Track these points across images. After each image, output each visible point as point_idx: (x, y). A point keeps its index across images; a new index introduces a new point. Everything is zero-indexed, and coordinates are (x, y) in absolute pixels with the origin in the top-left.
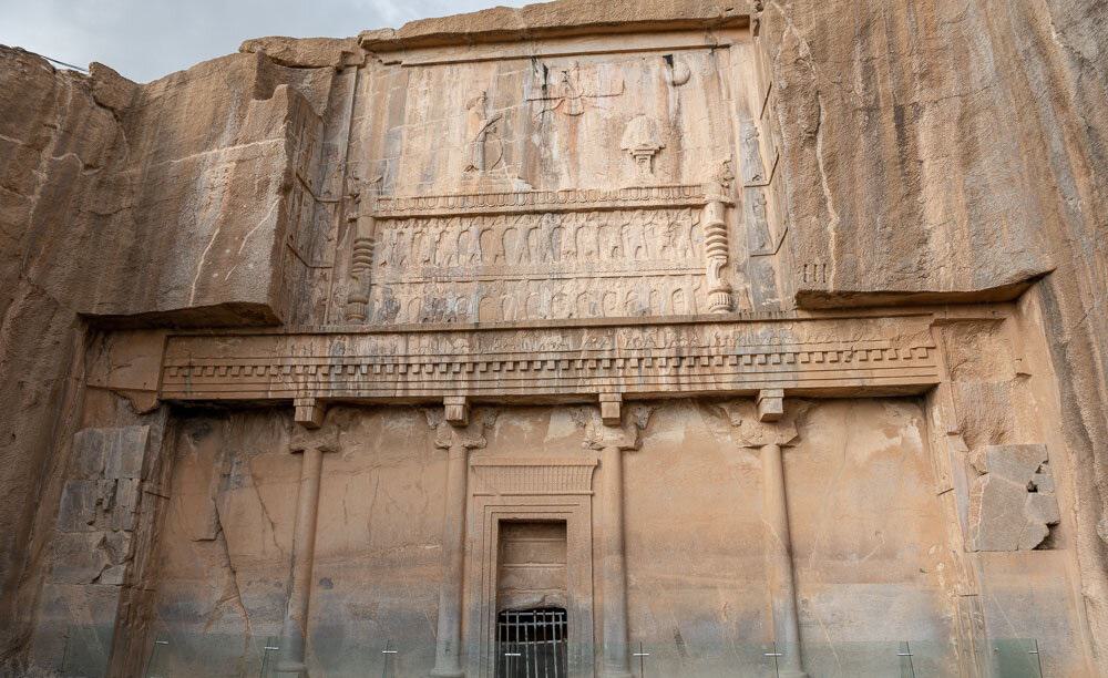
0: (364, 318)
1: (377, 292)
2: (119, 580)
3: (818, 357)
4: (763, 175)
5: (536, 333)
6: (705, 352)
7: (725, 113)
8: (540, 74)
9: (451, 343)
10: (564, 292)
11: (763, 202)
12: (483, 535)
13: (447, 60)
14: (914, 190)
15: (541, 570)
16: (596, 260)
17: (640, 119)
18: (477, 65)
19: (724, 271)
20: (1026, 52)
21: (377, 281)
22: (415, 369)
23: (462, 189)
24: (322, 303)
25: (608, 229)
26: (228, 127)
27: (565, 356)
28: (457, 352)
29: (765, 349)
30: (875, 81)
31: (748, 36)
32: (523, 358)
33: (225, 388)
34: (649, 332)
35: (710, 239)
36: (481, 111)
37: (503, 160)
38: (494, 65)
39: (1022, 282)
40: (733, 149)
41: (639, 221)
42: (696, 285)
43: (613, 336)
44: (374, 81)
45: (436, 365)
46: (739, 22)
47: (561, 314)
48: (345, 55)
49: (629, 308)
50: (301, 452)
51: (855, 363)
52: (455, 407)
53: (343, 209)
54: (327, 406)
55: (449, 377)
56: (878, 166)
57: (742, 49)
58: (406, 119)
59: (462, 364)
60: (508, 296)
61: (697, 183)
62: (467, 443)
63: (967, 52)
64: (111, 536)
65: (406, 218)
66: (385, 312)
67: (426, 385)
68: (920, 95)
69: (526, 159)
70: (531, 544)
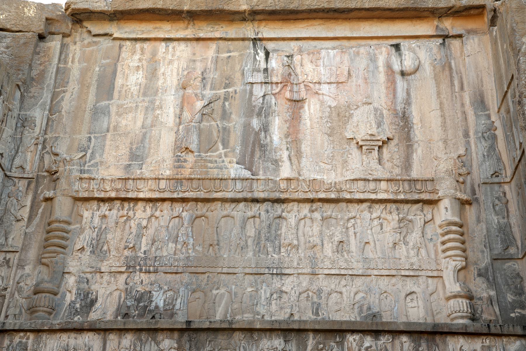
0: (52, 310)
1: (71, 281)
4: (503, 172)
5: (256, 336)
7: (458, 105)
9: (158, 344)
10: (284, 289)
11: (504, 201)
13: (162, 36)
17: (367, 107)
18: (194, 43)
19: (462, 273)
21: (71, 269)
23: (175, 172)
34: (384, 340)
35: (446, 237)
38: (213, 46)
40: (468, 143)
41: (366, 215)
42: (431, 288)
43: (341, 344)
44: (80, 52)
47: (276, 313)
49: (356, 310)
53: (37, 187)
57: (476, 40)
58: (116, 94)
60: (222, 291)
61: (428, 175)
65: (110, 200)
66: (78, 306)
69: (245, 142)
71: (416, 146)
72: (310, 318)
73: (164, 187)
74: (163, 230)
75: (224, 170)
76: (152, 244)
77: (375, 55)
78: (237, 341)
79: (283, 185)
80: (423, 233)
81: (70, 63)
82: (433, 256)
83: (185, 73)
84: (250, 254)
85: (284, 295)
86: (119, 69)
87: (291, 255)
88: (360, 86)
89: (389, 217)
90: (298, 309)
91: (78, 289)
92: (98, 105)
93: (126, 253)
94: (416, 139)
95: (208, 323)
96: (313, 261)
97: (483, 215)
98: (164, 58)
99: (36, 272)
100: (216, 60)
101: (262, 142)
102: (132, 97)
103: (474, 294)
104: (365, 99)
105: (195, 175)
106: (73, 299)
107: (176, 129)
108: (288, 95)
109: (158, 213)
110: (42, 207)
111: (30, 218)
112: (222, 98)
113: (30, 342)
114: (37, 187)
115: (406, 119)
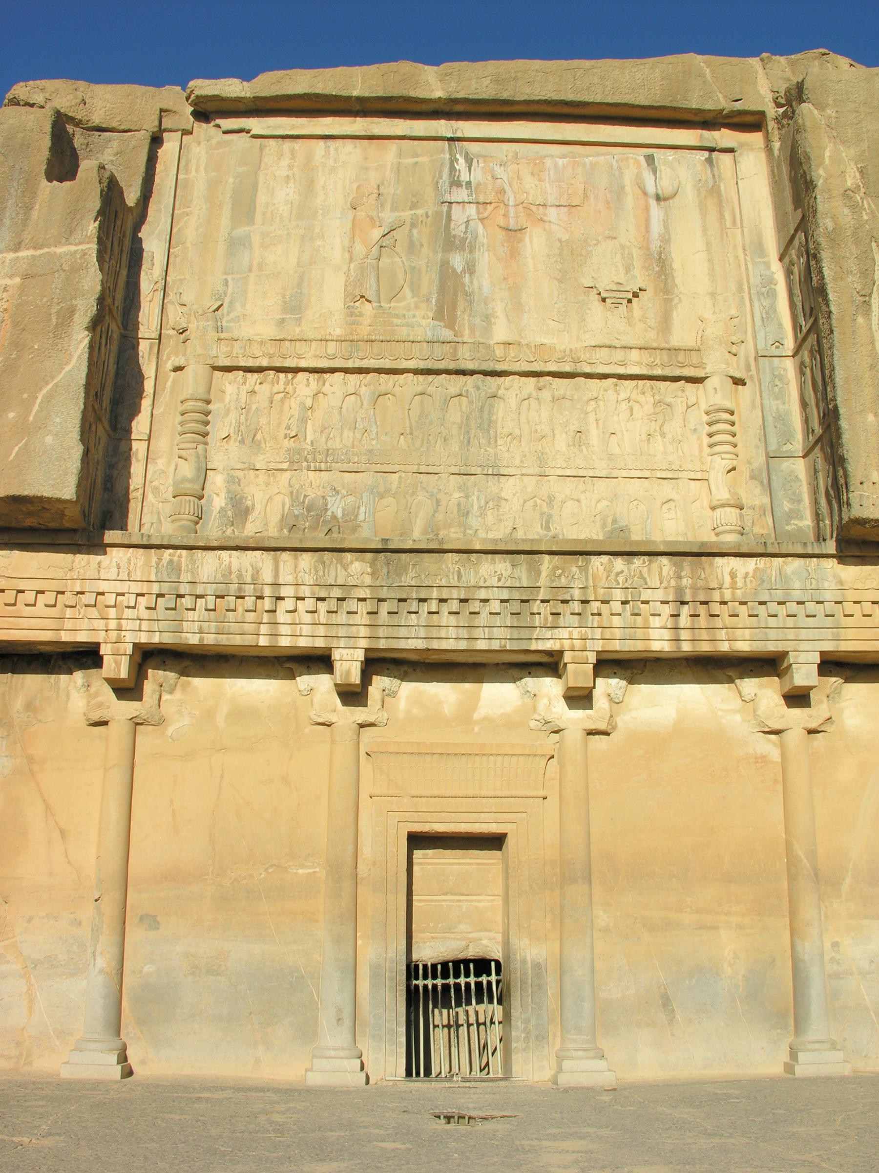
1: (217, 481)
6: (716, 596)
8: (462, 161)
9: (345, 567)
10: (503, 495)
15: (464, 906)
27: (516, 595)
29: (797, 595)
32: (455, 594)
38: (393, 145)
41: (611, 395)
43: (584, 569)
46: (748, 119)
49: (598, 524)
65: (260, 370)
66: (230, 513)
67: (306, 630)
71: (676, 300)
72: (538, 533)
73: (333, 352)
74: (336, 412)
75: (416, 328)
76: (322, 432)
77: (619, 168)
78: (450, 565)
79: (499, 352)
80: (684, 421)
81: (194, 173)
83: (355, 186)
84: (455, 448)
85: (503, 503)
86: (261, 180)
87: (511, 449)
88: (600, 212)
89: (642, 398)
90: (522, 523)
91: (229, 492)
92: (234, 232)
93: (287, 444)
94: (676, 291)
95: (411, 542)
96: (541, 458)
100: (398, 168)
101: (467, 288)
103: (744, 502)
104: (607, 232)
105: (376, 335)
106: (223, 505)
107: (345, 268)
108: (501, 221)
109: (326, 388)
110: (171, 379)
112: (408, 223)
115: (663, 262)
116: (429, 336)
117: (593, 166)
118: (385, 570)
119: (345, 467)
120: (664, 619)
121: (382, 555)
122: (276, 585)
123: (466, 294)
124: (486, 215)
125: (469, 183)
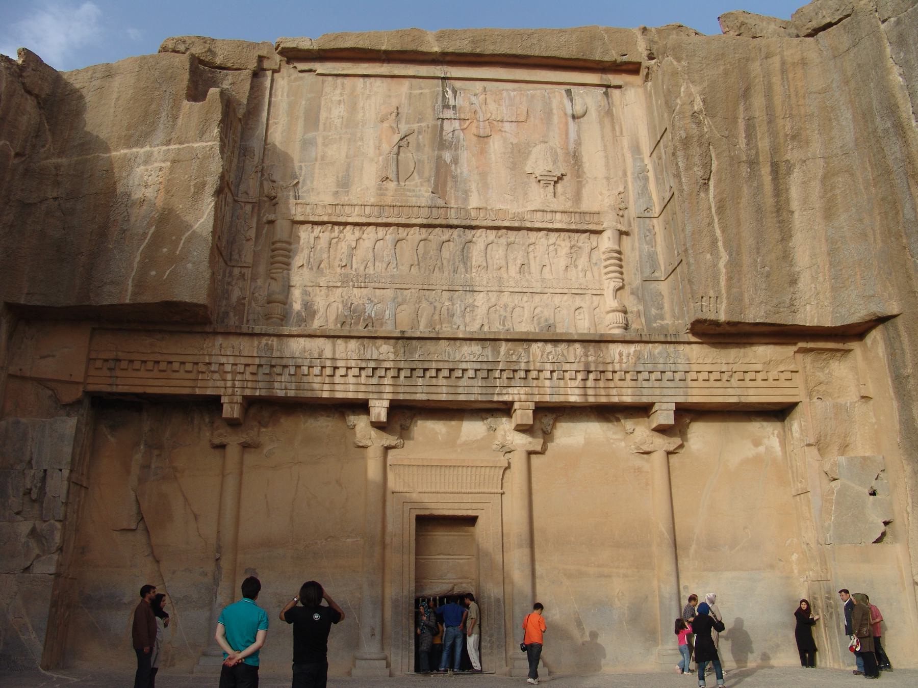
1: (296, 293)
2: (53, 569)
3: (704, 375)
5: (458, 342)
6: (610, 368)
8: (450, 92)
10: (476, 303)
11: (653, 233)
12: (401, 527)
14: (786, 235)
16: (505, 276)
17: (543, 146)
18: (389, 80)
20: (886, 131)
22: (342, 371)
24: (241, 301)
25: (516, 246)
26: (161, 126)
27: (485, 366)
28: (382, 357)
29: (661, 367)
30: (756, 138)
31: (637, 80)
33: (151, 382)
34: (563, 346)
36: (394, 125)
37: (415, 174)
38: (407, 82)
39: (871, 321)
40: (626, 182)
42: (595, 304)
43: (527, 350)
45: (361, 369)
46: (631, 67)
48: (261, 59)
49: (535, 322)
50: (222, 447)
51: (734, 382)
52: (379, 410)
53: (259, 210)
54: (250, 403)
55: (375, 380)
56: (759, 210)
58: (321, 126)
59: (387, 369)
61: (595, 209)
62: (387, 443)
63: (830, 120)
64: (40, 526)
65: (323, 223)
67: (351, 388)
68: (792, 154)
70: (442, 536)
71: (584, 182)
74: (371, 251)
77: (549, 98)
79: (473, 213)
82: (597, 277)
84: (446, 273)
86: (323, 103)
89: (563, 244)
91: (303, 300)
96: (500, 280)
97: (637, 244)
98: (363, 94)
99: (267, 284)
100: (410, 96)
102: (336, 129)
109: (365, 236)
111: (257, 238)
113: (275, 343)
114: (259, 210)
116: (430, 203)
117: (533, 96)
118: (402, 351)
119: (377, 285)
120: (578, 383)
121: (400, 342)
122: (334, 359)
123: (453, 177)
124: (465, 126)
125: (454, 107)
